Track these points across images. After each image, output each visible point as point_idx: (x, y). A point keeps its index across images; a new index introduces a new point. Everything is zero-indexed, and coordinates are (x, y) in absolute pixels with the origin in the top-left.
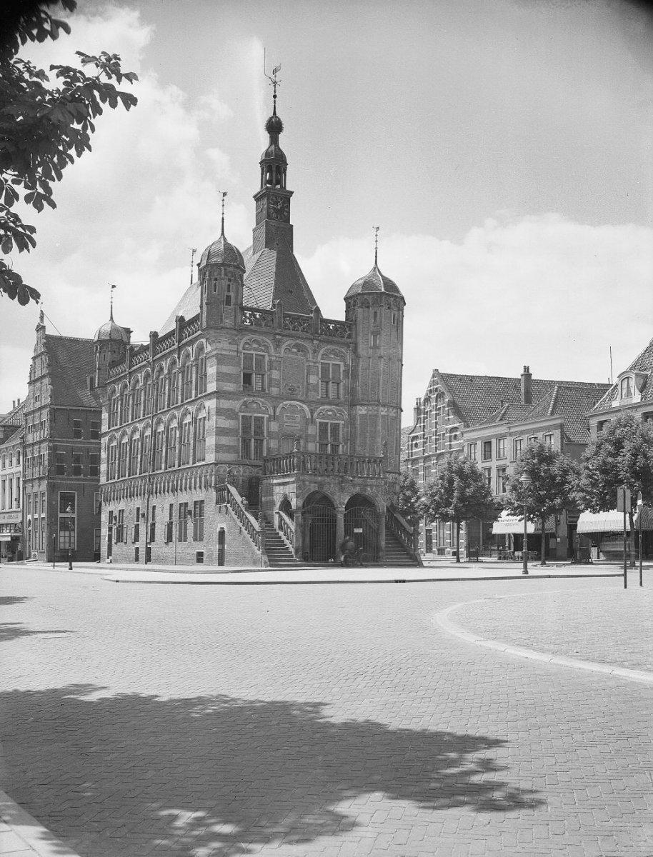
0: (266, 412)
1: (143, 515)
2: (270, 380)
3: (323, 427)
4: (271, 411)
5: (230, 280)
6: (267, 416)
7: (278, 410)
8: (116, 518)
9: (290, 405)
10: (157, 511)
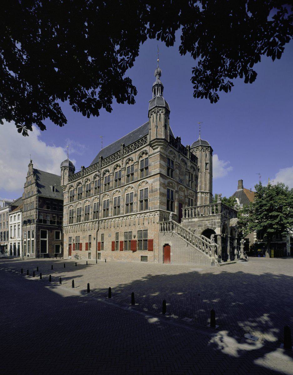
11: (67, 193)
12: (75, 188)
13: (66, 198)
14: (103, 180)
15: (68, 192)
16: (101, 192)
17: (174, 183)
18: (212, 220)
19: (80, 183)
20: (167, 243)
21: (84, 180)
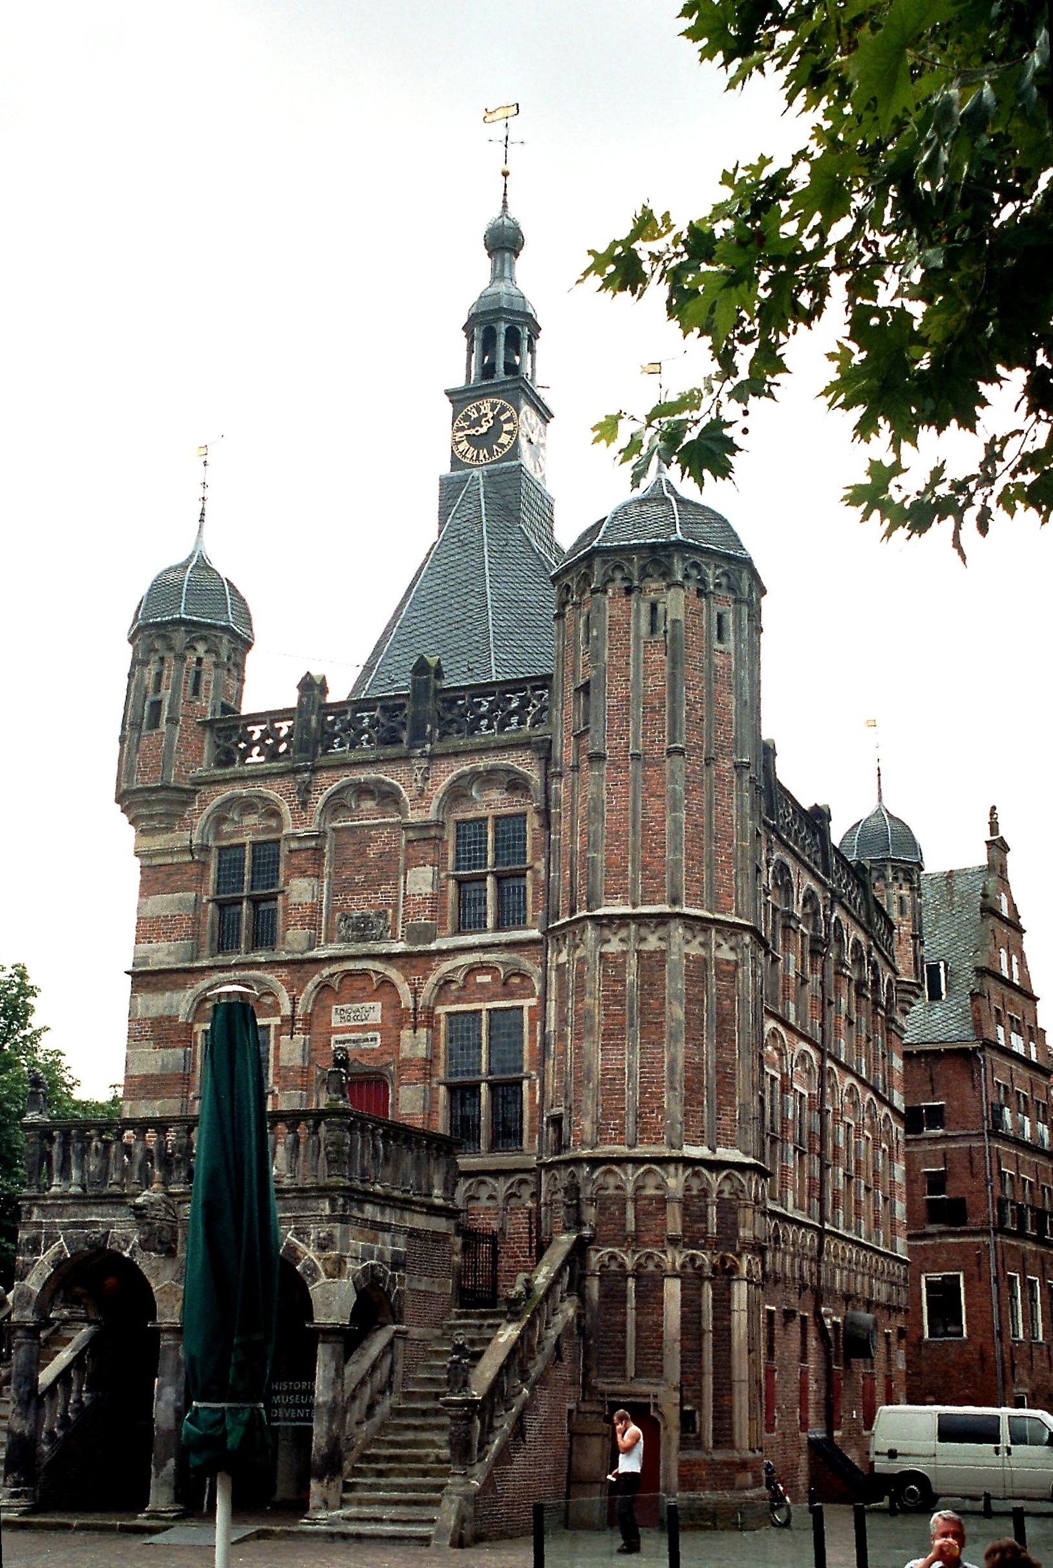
4: (286, 1010)
5: (162, 659)
6: (277, 1021)
9: (348, 974)
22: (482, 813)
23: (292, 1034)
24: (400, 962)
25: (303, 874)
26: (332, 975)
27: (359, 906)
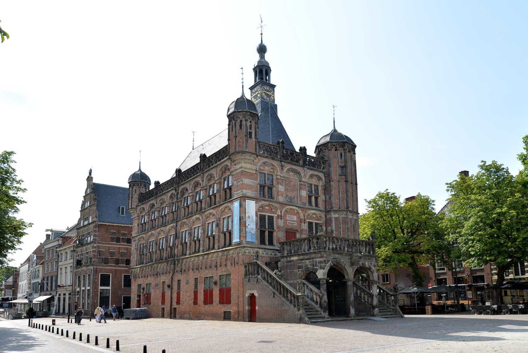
0: (275, 213)
1: (169, 286)
2: (278, 192)
3: (310, 224)
7: (283, 212)
8: (143, 289)
9: (290, 209)
10: (183, 284)
11: (136, 218)
12: (147, 211)
13: (135, 226)
14: (181, 201)
15: (138, 218)
16: (178, 219)
17: (272, 205)
18: (313, 258)
19: (153, 205)
20: (252, 292)
21: (158, 201)
22: (312, 183)
23: (281, 219)
24: (301, 209)
25: (281, 184)
26: (288, 208)
27: (290, 194)
